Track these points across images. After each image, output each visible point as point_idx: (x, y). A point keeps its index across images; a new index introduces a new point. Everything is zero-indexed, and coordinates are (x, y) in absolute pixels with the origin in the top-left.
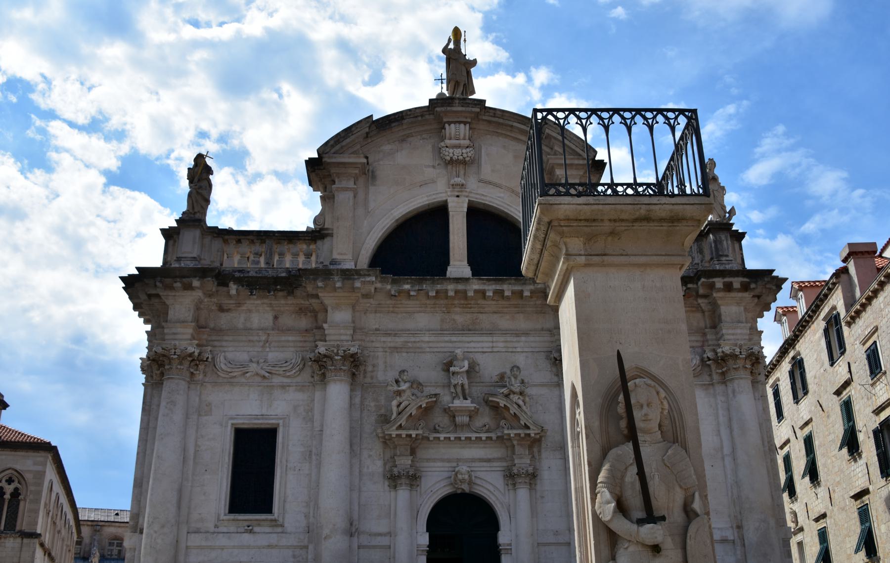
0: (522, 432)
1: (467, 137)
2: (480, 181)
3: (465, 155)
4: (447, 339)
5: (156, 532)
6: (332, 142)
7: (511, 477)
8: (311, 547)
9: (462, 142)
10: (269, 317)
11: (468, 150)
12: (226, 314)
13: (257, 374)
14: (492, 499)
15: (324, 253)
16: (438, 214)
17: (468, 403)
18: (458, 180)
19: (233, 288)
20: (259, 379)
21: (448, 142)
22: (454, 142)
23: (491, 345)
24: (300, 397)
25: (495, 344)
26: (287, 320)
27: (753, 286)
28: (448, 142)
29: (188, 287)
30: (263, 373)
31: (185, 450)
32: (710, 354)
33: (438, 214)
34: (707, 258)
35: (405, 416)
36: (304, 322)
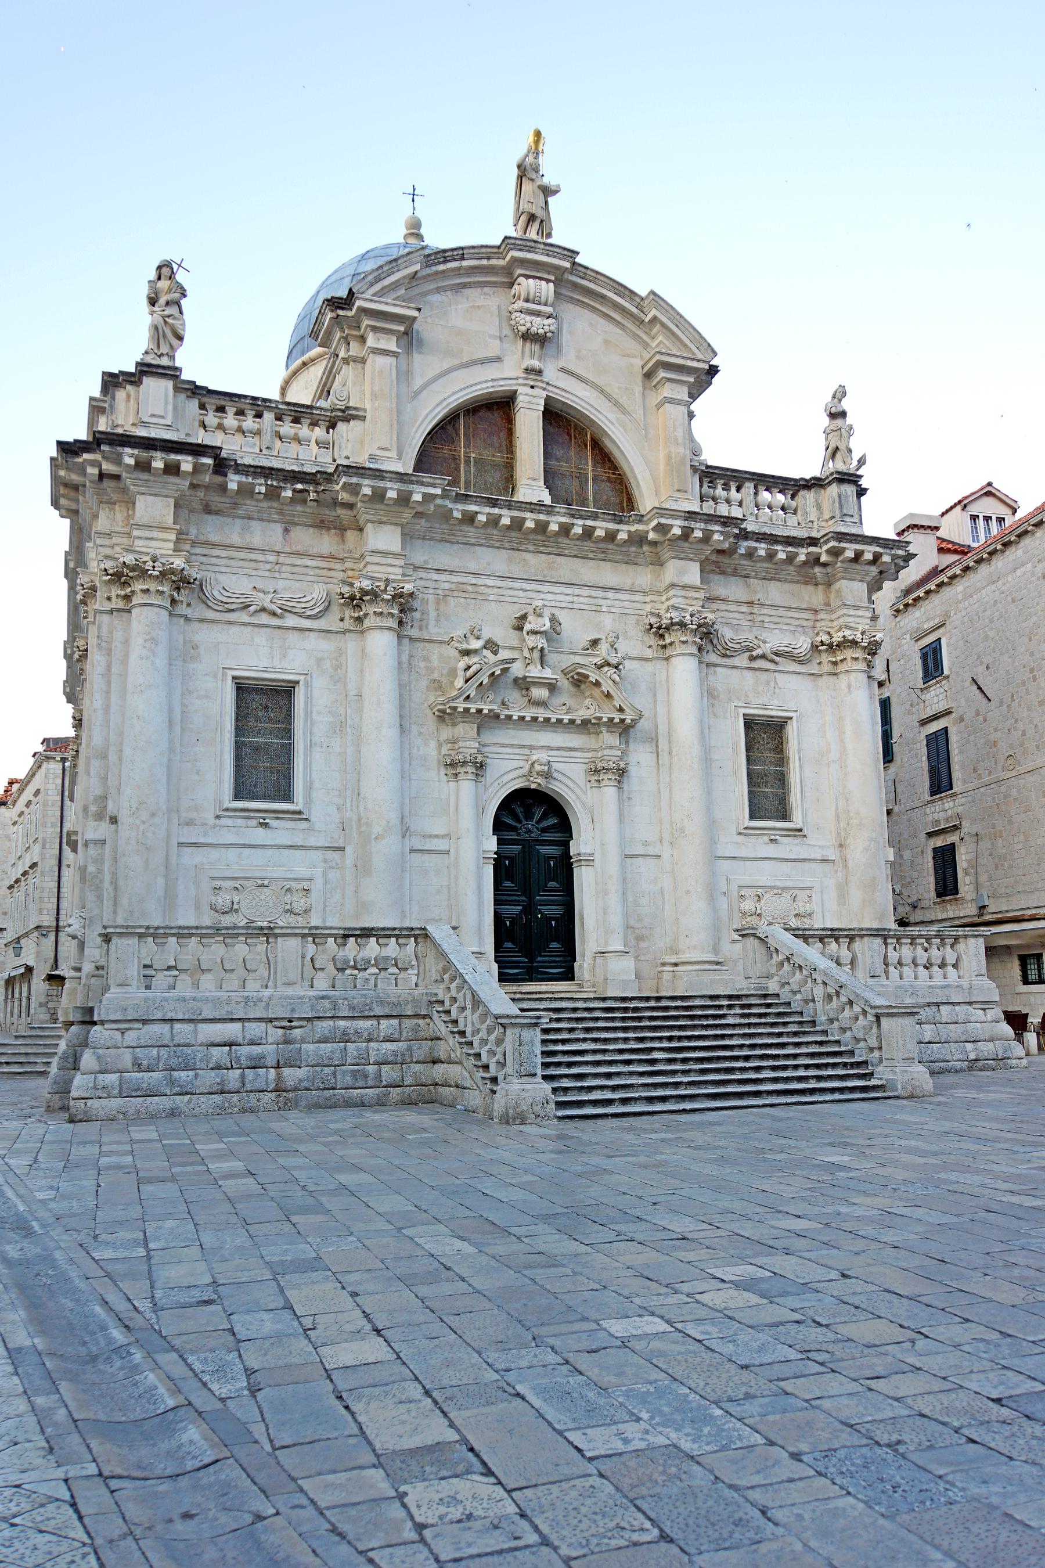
2: (563, 370)
3: (547, 328)
4: (517, 585)
5: (144, 822)
6: (370, 278)
8: (349, 849)
10: (278, 528)
11: (550, 321)
12: (214, 517)
13: (263, 609)
15: (352, 444)
16: (501, 406)
17: (547, 673)
18: (536, 364)
19: (233, 481)
20: (264, 619)
23: (571, 599)
24: (325, 646)
25: (576, 599)
26: (305, 538)
27: (886, 559)
29: (172, 469)
30: (274, 607)
31: (171, 710)
32: (825, 638)
33: (501, 406)
34: (826, 516)
35: (474, 683)
36: (326, 543)
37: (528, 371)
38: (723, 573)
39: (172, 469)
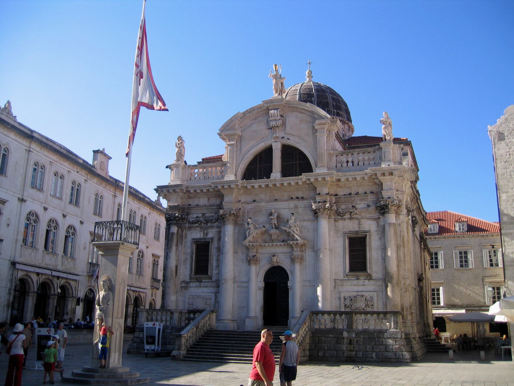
0: (295, 242)
1: (279, 115)
7: (293, 260)
9: (277, 118)
10: (207, 199)
14: (286, 268)
21: (271, 119)
22: (273, 118)
28: (271, 119)
37: (275, 138)
38: (341, 187)
39: (174, 191)
